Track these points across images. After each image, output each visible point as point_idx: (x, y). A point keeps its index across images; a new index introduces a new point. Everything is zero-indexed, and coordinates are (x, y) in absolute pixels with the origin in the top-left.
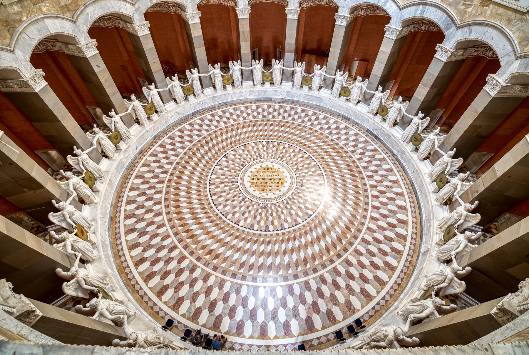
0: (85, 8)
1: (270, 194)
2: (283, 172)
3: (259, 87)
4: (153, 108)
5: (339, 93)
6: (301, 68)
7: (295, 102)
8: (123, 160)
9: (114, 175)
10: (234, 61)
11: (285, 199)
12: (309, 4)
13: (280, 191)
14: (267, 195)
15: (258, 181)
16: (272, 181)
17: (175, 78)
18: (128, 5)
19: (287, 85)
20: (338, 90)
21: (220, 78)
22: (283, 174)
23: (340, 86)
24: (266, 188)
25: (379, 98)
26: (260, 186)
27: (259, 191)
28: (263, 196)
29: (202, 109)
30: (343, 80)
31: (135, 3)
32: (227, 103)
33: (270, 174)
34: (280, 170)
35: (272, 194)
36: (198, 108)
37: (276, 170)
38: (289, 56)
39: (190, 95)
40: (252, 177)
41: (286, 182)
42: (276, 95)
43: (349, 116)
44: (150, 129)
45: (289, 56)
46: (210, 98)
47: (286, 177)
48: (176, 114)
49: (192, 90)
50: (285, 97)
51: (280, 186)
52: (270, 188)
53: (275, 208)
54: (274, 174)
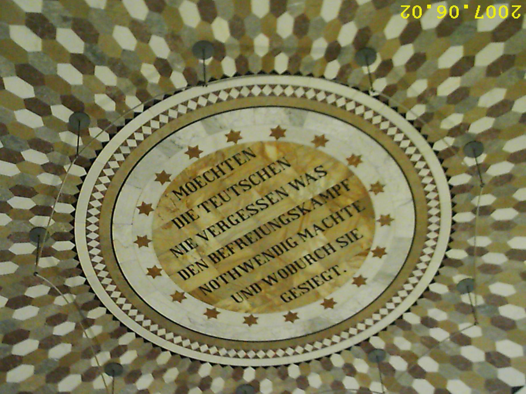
1: (337, 296)
2: (321, 141)
11: (437, 277)
13: (380, 252)
14: (329, 304)
15: (226, 265)
16: (295, 226)
22: (328, 149)
24: (298, 279)
26: (256, 288)
27: (272, 308)
28: (312, 322)
33: (254, 195)
34: (289, 138)
35: (349, 287)
37: (272, 153)
40: (176, 266)
41: (378, 188)
47: (355, 160)
51: (363, 230)
52: (316, 268)
53: (412, 341)
54: (272, 182)
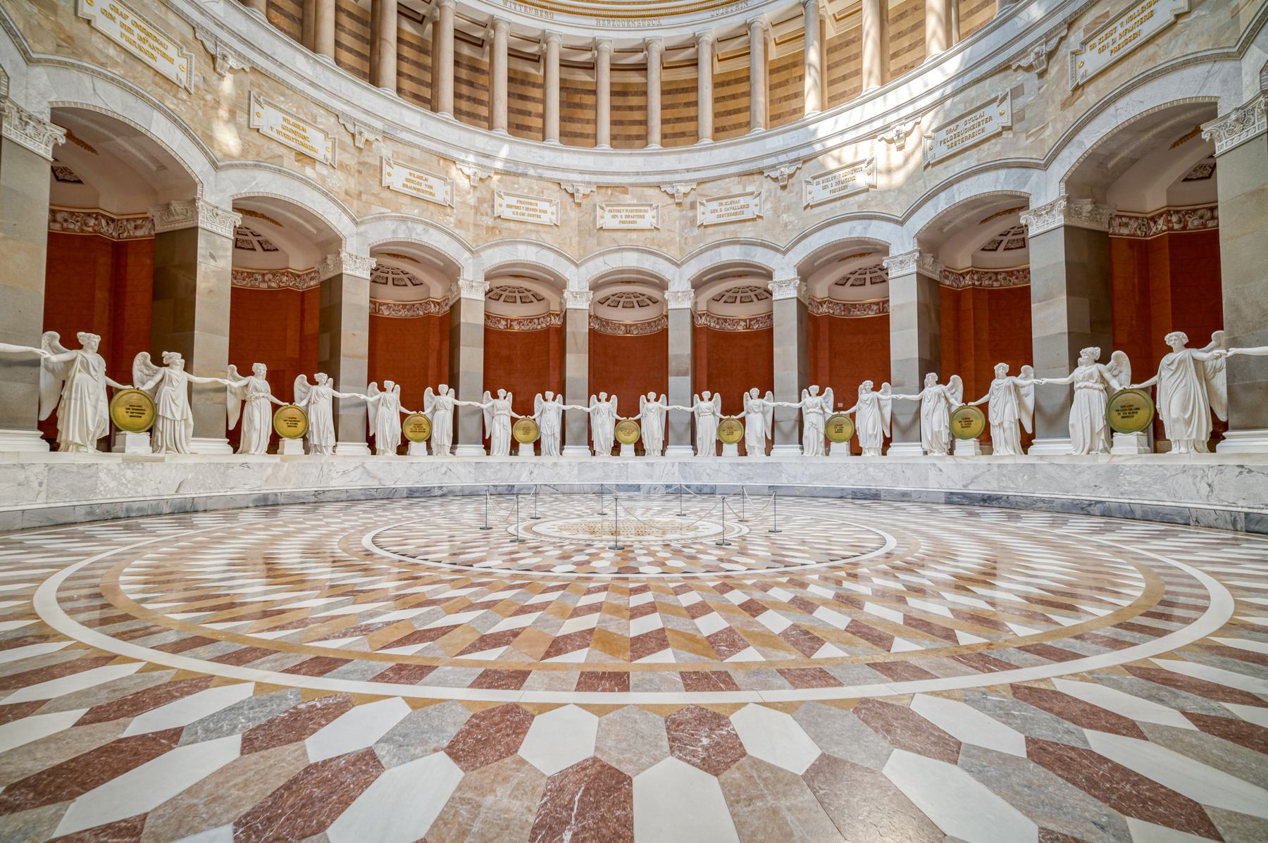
0: (255, 165)
3: (605, 457)
4: (301, 425)
5: (822, 437)
6: (711, 403)
7: (705, 490)
8: (102, 475)
9: (21, 476)
10: (547, 393)
12: (712, 324)
17: (393, 392)
18: (346, 219)
19: (680, 452)
20: (818, 433)
21: (508, 422)
23: (821, 418)
25: (939, 397)
29: (441, 488)
30: (824, 404)
31: (362, 222)
32: (515, 490)
36: (430, 481)
38: (680, 383)
39: (418, 441)
42: (651, 477)
43: (873, 486)
44: (261, 465)
45: (680, 383)
46: (469, 463)
48: (360, 470)
49: (427, 430)
50: (677, 481)
